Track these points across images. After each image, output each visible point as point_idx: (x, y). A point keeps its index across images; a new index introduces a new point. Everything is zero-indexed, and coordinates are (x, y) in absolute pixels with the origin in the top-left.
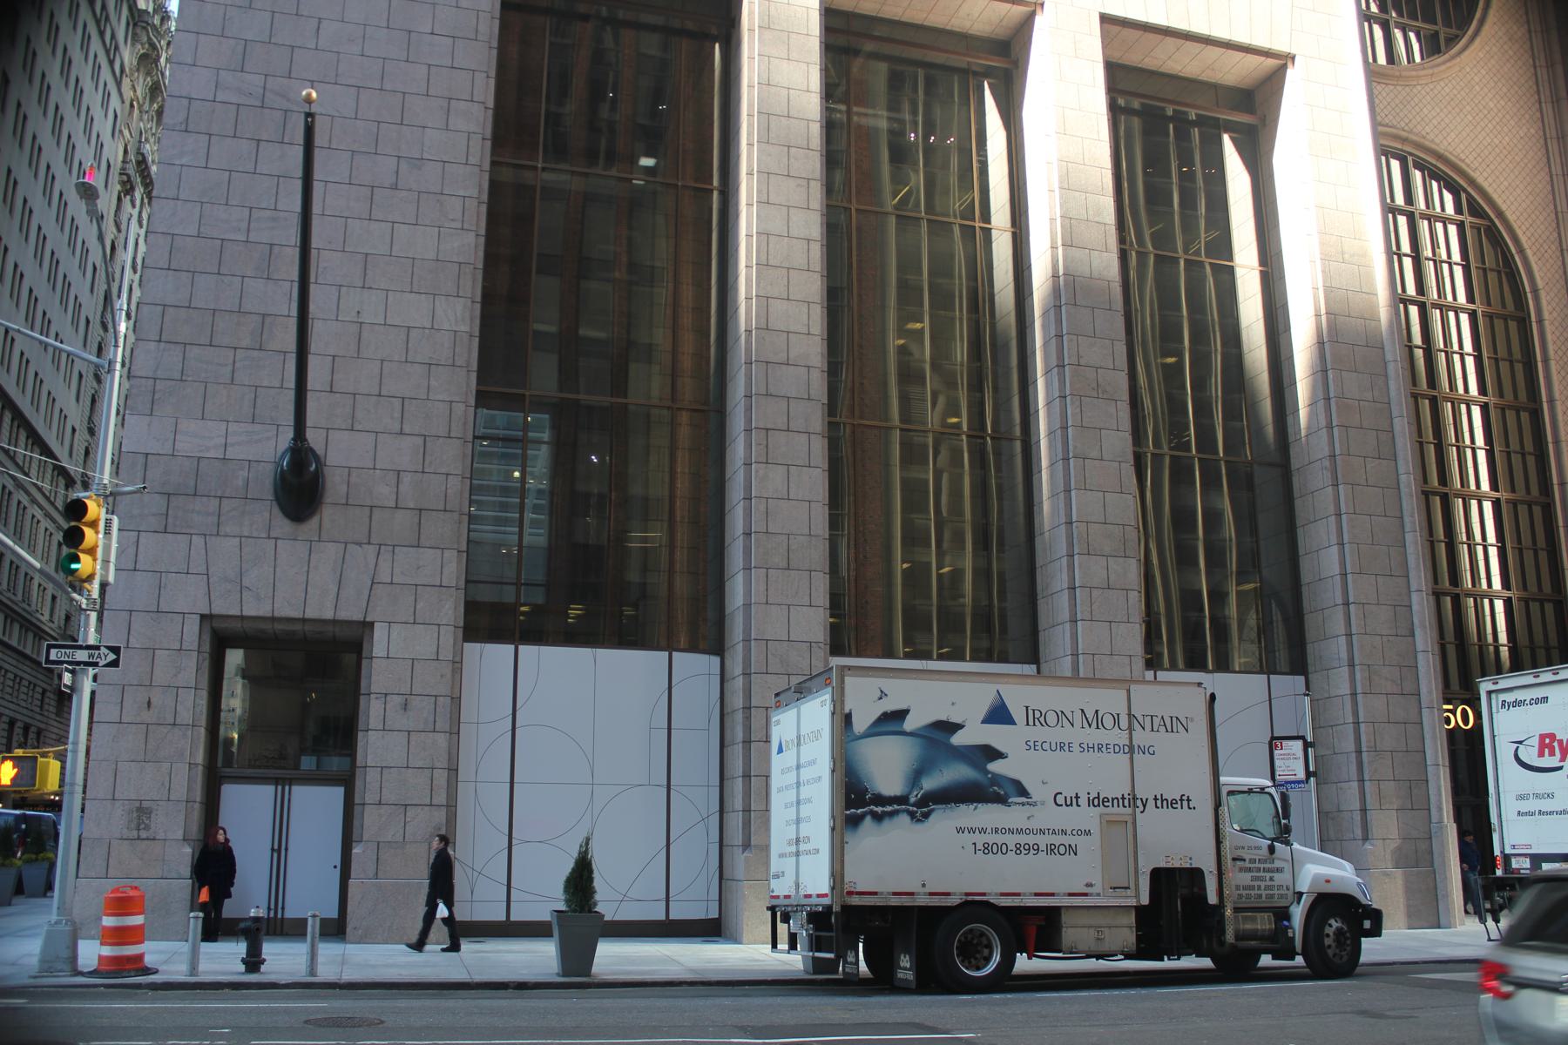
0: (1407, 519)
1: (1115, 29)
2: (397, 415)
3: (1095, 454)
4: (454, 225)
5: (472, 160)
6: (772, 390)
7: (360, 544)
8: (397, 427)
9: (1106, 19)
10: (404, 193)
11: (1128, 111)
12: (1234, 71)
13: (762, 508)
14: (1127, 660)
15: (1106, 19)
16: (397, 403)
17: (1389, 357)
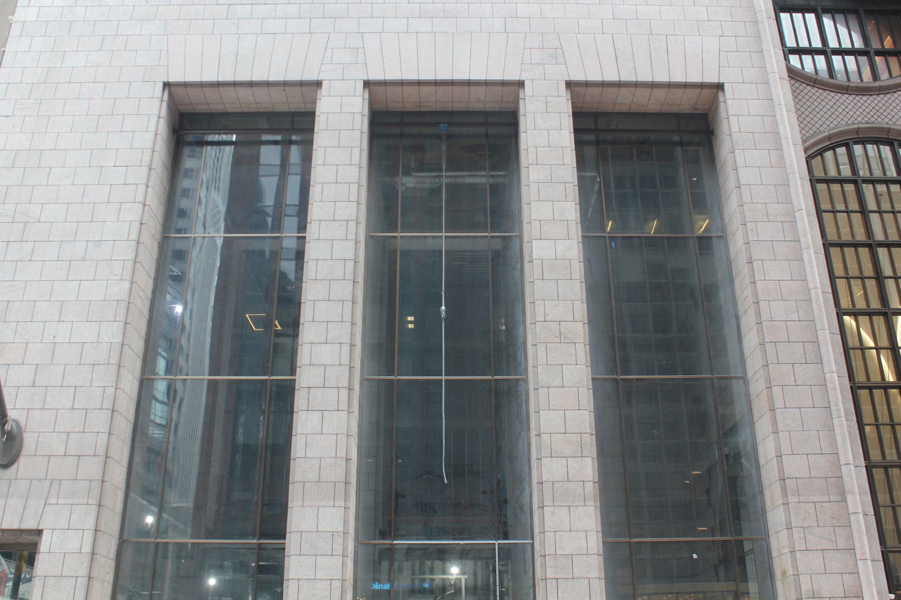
0: (833, 408)
1: (582, 90)
2: (71, 397)
3: (558, 383)
4: (117, 278)
5: (132, 237)
6: (314, 361)
7: (40, 480)
8: (70, 405)
9: (569, 84)
10: (89, 262)
11: (588, 143)
12: (684, 103)
13: (303, 441)
14: (583, 535)
15: (569, 84)
16: (72, 390)
17: (811, 286)
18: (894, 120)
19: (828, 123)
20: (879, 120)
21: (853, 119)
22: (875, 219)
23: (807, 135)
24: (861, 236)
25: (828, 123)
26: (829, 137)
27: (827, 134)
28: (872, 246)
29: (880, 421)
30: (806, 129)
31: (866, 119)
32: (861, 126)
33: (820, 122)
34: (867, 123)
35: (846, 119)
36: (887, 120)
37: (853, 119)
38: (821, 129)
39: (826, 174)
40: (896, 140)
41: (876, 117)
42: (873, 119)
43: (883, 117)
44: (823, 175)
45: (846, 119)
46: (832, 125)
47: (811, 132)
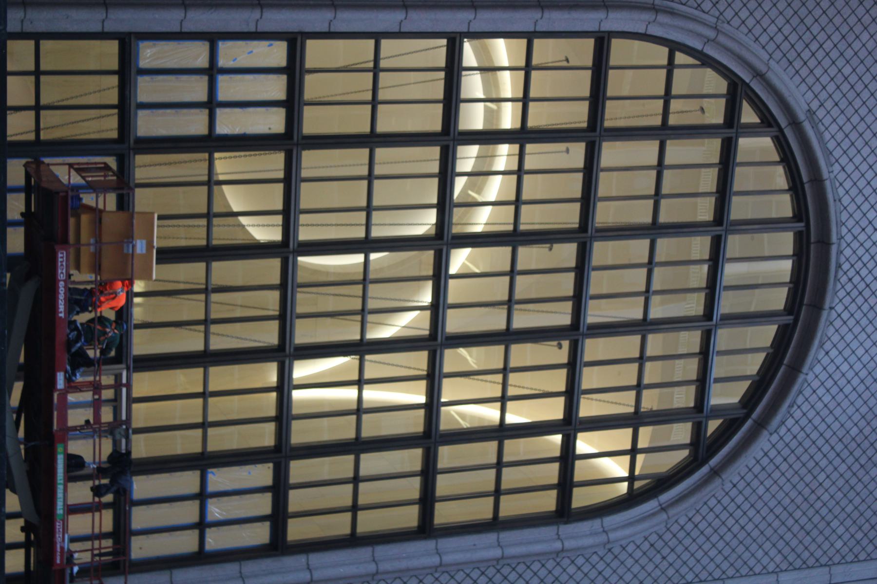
18: (838, 323)
19: (848, 184)
20: (841, 294)
21: (849, 238)
22: (629, 345)
23: (827, 136)
24: (596, 313)
25: (848, 184)
26: (817, 180)
27: (825, 175)
28: (575, 332)
29: (214, 297)
30: (840, 136)
31: (846, 266)
32: (834, 250)
33: (850, 168)
34: (839, 266)
35: (851, 223)
36: (839, 308)
37: (849, 238)
38: (836, 168)
39: (717, 380)
40: (796, 320)
41: (849, 287)
42: (844, 279)
43: (847, 301)
44: (724, 283)
45: (851, 223)
46: (841, 191)
47: (831, 145)
